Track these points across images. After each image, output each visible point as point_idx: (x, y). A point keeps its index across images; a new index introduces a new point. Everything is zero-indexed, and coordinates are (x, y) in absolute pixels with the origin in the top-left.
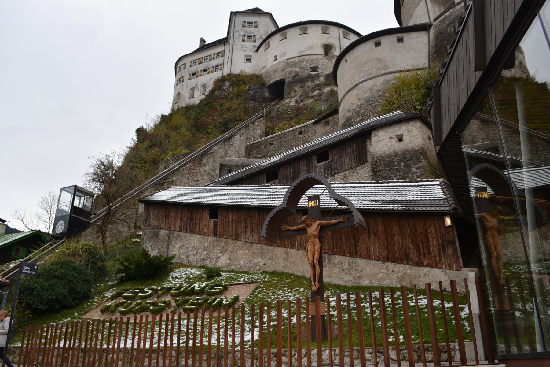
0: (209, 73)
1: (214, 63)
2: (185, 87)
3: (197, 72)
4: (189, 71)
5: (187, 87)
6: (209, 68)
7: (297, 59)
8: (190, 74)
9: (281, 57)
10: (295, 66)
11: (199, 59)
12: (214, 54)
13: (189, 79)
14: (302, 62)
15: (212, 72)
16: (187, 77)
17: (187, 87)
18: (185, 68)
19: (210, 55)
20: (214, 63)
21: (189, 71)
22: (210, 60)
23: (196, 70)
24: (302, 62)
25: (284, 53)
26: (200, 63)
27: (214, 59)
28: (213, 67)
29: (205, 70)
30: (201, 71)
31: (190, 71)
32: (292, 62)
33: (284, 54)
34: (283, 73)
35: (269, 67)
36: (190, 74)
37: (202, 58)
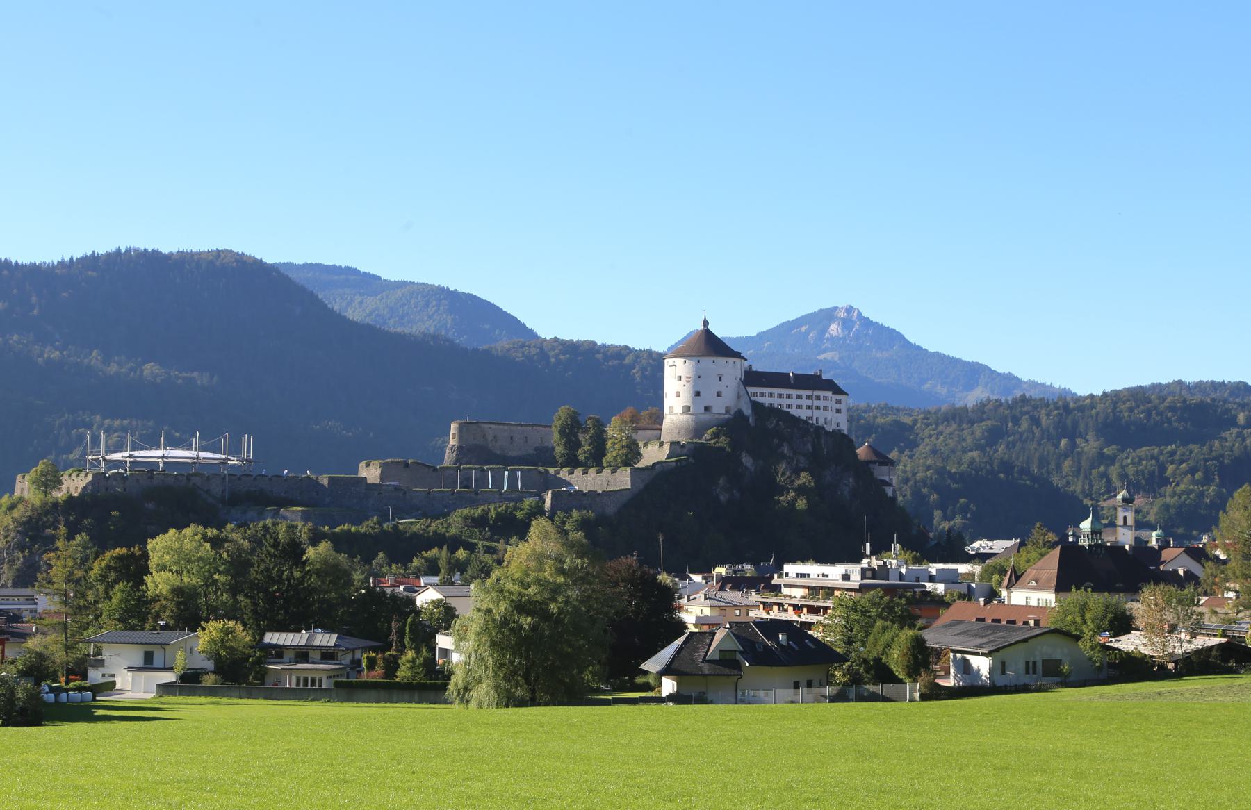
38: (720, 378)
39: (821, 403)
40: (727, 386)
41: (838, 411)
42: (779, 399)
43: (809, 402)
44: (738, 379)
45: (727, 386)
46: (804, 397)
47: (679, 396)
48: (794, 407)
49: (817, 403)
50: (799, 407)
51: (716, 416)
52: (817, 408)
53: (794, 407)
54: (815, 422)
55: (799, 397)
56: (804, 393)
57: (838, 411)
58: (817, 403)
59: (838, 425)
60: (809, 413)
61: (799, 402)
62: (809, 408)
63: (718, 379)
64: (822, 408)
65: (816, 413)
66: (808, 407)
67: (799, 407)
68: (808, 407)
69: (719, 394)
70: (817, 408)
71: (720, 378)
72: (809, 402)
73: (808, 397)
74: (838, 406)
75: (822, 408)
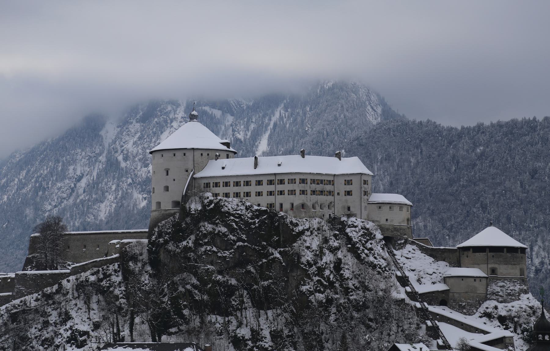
0: (325, 195)
1: (328, 188)
2: (309, 200)
3: (317, 191)
4: (310, 187)
5: (310, 201)
6: (324, 191)
7: (398, 227)
8: (311, 191)
9: (391, 222)
10: (398, 231)
11: (317, 180)
12: (327, 180)
13: (311, 195)
14: (401, 229)
15: (327, 195)
16: (309, 192)
17: (310, 201)
18: (307, 183)
19: (325, 180)
20: (328, 188)
21: (310, 187)
22: (325, 184)
23: (316, 189)
24: (401, 229)
25: (392, 220)
26: (318, 184)
27: (327, 185)
28: (327, 191)
29: (322, 192)
30: (319, 191)
31: (311, 188)
32: (396, 228)
33: (392, 221)
34: (393, 233)
35: (383, 224)
36: (311, 191)
37: (319, 180)
40: (174, 180)
41: (349, 193)
42: (246, 187)
43: (271, 188)
45: (174, 180)
47: (168, 190)
49: (280, 187)
50: (259, 194)
51: (163, 212)
52: (281, 193)
53: (253, 194)
57: (349, 193)
58: (280, 187)
59: (349, 209)
60: (271, 199)
61: (259, 188)
62: (271, 195)
63: (165, 173)
64: (286, 193)
65: (279, 199)
66: (271, 193)
67: (259, 194)
68: (271, 193)
69: (167, 189)
70: (281, 193)
72: (271, 188)
74: (348, 188)
75: (286, 193)
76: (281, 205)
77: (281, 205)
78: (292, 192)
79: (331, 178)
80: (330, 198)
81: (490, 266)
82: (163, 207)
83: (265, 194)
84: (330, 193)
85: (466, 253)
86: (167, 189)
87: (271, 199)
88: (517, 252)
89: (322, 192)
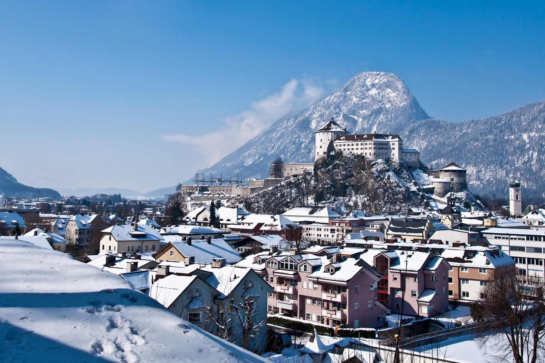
1: (385, 146)
20: (385, 146)
38: (321, 140)
39: (368, 146)
43: (362, 147)
44: (330, 140)
46: (346, 145)
48: (355, 149)
49: (366, 146)
50: (357, 149)
52: (366, 148)
53: (355, 149)
54: (365, 155)
55: (357, 145)
56: (359, 143)
60: (362, 151)
61: (357, 147)
62: (362, 149)
65: (366, 151)
66: (362, 149)
67: (357, 149)
68: (362, 149)
69: (321, 147)
70: (366, 148)
71: (321, 140)
72: (362, 147)
73: (362, 144)
75: (368, 148)
76: (366, 153)
77: (366, 153)
78: (370, 148)
79: (387, 143)
80: (386, 151)
81: (451, 178)
82: (320, 154)
83: (360, 149)
84: (386, 149)
85: (441, 172)
86: (321, 147)
87: (362, 151)
88: (462, 172)
89: (382, 148)
